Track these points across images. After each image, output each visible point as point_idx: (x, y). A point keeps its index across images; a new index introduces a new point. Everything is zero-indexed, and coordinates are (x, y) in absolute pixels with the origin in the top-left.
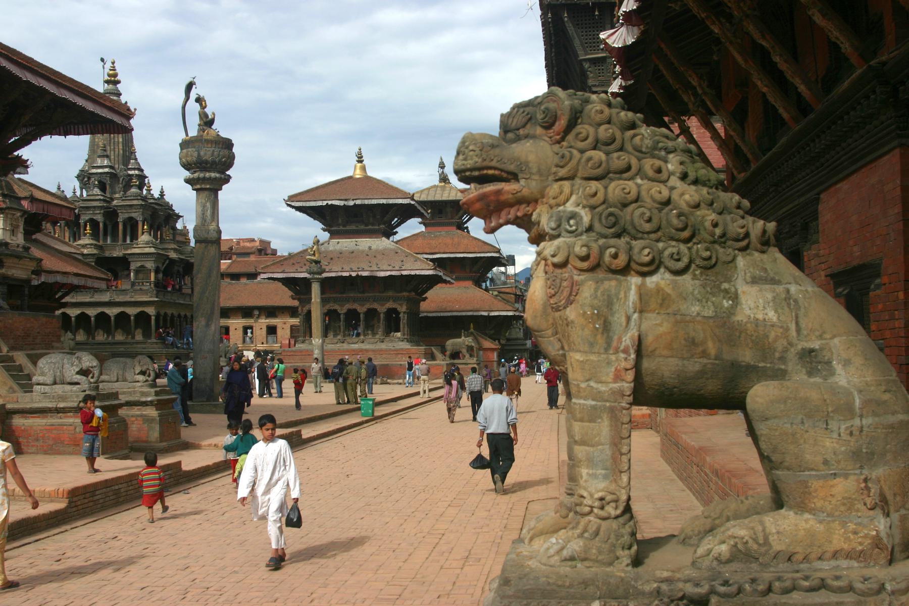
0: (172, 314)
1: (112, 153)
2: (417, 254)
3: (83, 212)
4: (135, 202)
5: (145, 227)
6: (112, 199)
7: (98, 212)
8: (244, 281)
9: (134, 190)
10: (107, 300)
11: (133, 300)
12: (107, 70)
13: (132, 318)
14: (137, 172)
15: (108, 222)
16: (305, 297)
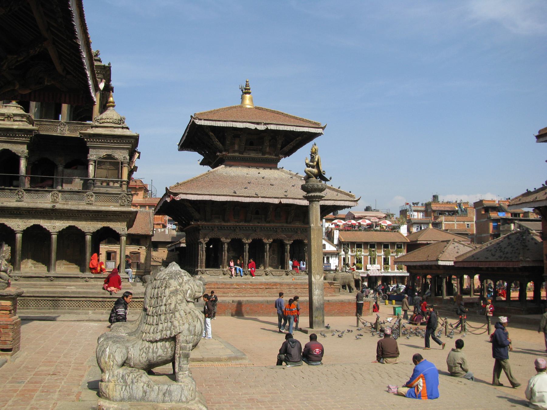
10: (49, 206)
11: (93, 208)
13: (88, 237)
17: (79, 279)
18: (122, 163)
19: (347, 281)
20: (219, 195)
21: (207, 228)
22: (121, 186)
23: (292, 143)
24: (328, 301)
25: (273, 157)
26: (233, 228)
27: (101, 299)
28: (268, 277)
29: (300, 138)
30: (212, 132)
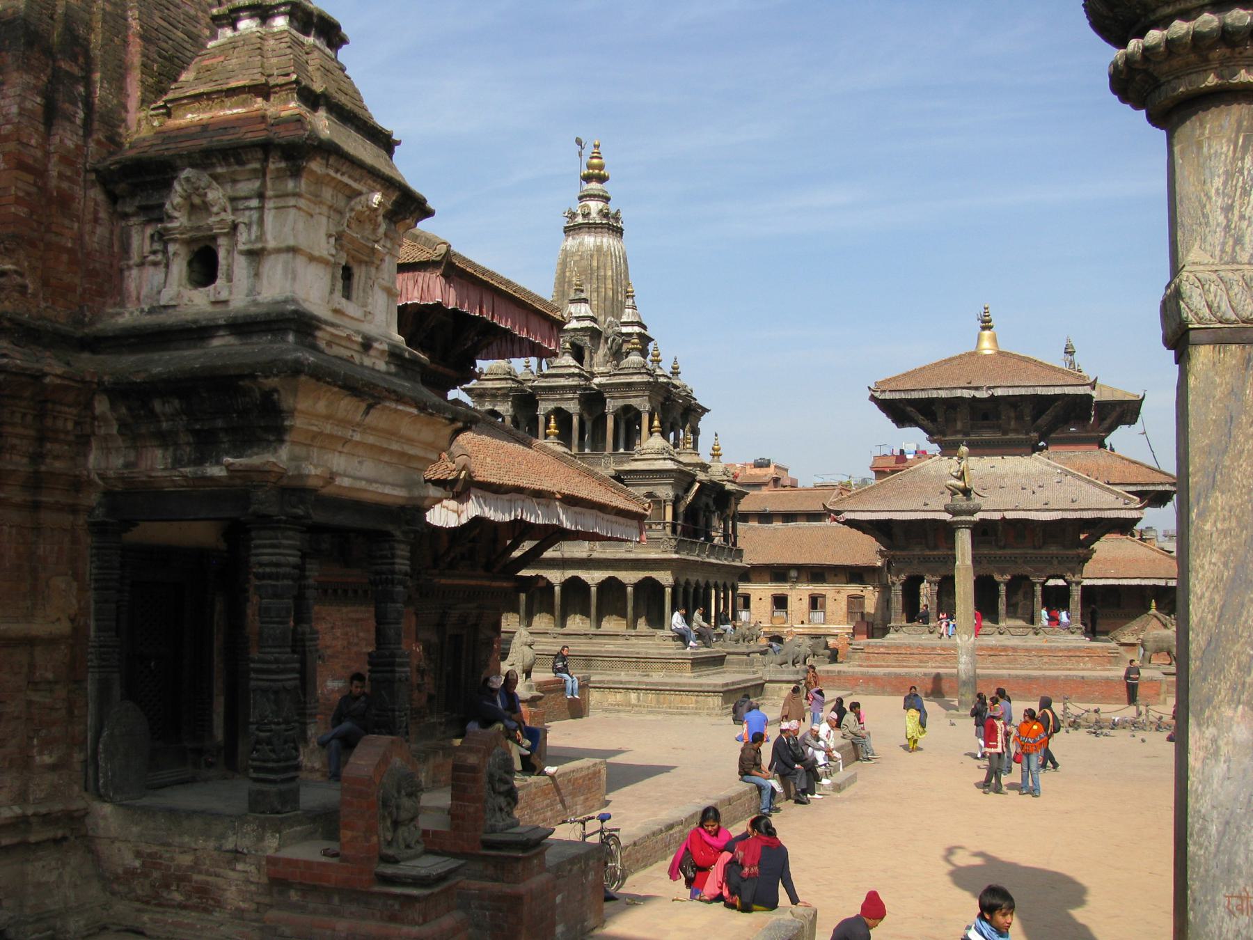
0: (697, 583)
1: (595, 294)
2: (1108, 484)
3: (544, 397)
4: (636, 379)
5: (656, 423)
6: (593, 375)
7: (570, 396)
8: (777, 525)
9: (635, 358)
10: (584, 555)
11: (632, 556)
12: (586, 159)
13: (630, 589)
14: (637, 329)
15: (586, 416)
16: (904, 553)
17: (619, 637)
18: (665, 502)
19: (1165, 645)
20: (904, 511)
21: (901, 560)
22: (664, 528)
23: (1048, 412)
24: (1083, 677)
25: (1021, 436)
26: (944, 558)
27: (634, 660)
28: (1002, 637)
29: (1060, 403)
30: (912, 406)
